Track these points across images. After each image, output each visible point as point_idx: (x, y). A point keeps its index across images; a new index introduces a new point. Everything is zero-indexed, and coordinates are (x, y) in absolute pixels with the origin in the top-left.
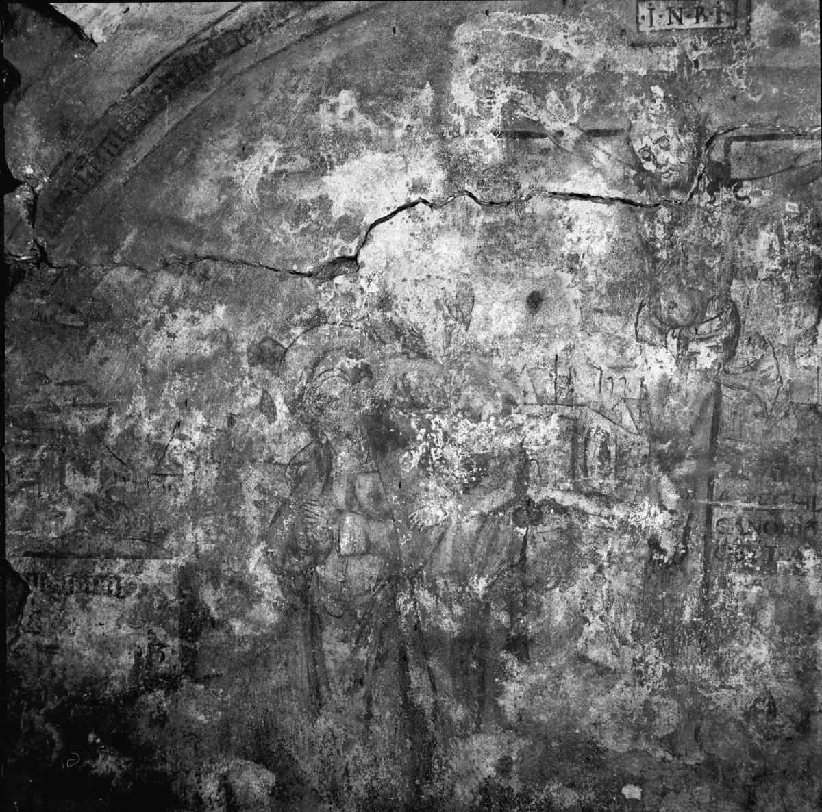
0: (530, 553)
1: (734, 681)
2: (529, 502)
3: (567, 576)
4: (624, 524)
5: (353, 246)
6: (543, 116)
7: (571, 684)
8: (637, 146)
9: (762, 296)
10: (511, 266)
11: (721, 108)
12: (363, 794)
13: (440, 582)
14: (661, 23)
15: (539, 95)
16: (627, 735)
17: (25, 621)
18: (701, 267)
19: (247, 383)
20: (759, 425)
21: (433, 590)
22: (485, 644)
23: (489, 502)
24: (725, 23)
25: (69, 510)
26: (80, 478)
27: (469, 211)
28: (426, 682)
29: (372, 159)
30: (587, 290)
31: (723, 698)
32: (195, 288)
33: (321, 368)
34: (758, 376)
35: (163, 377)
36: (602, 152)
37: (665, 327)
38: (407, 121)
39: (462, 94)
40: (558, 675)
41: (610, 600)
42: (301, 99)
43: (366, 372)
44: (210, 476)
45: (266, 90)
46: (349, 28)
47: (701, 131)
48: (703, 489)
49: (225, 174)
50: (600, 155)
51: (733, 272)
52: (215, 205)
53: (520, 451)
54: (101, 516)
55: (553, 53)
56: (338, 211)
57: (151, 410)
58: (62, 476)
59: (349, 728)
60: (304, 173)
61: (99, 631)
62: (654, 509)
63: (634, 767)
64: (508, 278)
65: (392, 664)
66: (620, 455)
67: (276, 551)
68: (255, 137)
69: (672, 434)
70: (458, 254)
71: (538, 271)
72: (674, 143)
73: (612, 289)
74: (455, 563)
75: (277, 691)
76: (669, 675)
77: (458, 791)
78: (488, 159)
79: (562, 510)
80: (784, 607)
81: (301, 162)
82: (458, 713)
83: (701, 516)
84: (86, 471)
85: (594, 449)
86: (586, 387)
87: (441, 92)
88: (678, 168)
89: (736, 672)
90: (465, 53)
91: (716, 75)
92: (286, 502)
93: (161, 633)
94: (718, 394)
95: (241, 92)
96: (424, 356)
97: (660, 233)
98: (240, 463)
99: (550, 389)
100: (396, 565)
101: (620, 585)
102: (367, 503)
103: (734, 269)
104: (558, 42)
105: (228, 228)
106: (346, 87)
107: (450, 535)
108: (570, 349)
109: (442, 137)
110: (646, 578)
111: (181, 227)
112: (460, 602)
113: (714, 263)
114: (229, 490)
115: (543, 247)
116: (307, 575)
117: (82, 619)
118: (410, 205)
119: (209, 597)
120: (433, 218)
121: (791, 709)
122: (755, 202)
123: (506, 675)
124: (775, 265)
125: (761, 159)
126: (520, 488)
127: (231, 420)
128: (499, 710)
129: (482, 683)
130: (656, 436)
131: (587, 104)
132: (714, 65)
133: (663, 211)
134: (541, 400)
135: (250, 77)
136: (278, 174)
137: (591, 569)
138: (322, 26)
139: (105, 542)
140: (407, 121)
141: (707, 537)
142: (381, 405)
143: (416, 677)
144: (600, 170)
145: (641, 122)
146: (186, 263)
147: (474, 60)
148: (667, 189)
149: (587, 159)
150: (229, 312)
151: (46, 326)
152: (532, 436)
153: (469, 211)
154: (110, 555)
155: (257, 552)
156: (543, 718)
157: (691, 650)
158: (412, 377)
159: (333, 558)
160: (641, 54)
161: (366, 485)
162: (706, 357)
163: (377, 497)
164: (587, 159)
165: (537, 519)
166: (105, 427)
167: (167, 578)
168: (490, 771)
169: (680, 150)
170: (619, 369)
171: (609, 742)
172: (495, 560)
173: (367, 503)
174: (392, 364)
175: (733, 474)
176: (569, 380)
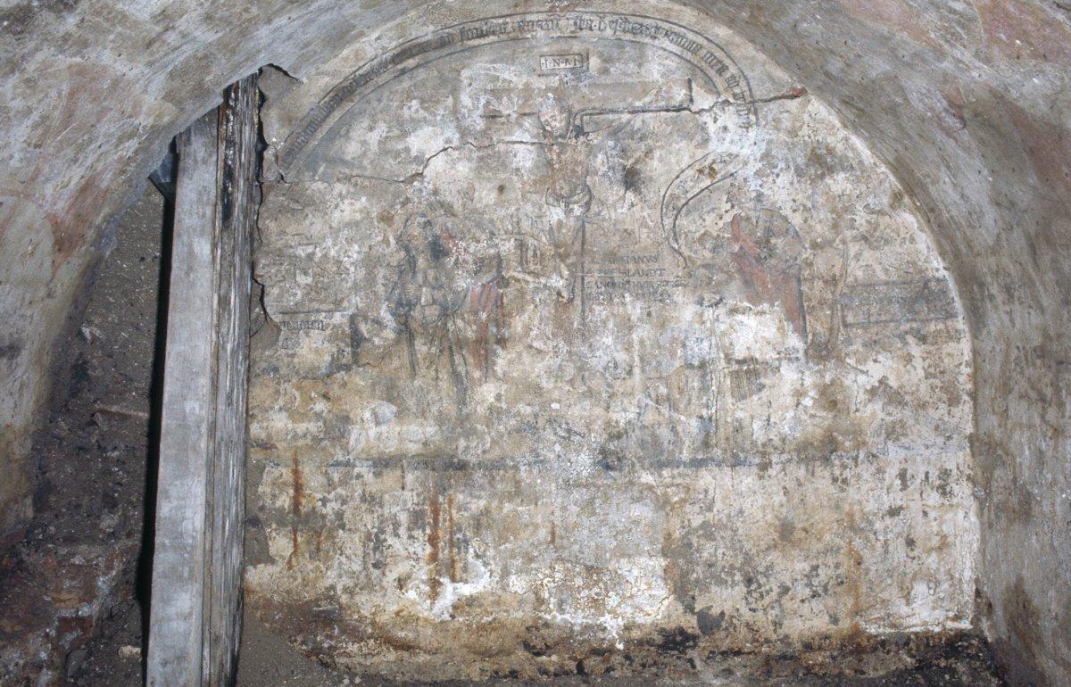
0: (505, 300)
1: (598, 354)
2: (503, 278)
3: (521, 310)
4: (545, 286)
5: (421, 168)
6: (501, 108)
7: (527, 359)
8: (543, 120)
9: (601, 183)
10: (490, 174)
11: (578, 102)
12: (437, 414)
13: (466, 316)
14: (550, 65)
15: (499, 99)
16: (553, 380)
17: (280, 343)
18: (573, 171)
19: (377, 231)
20: (602, 240)
21: (463, 319)
22: (486, 343)
23: (485, 279)
24: (578, 65)
25: (299, 292)
26: (303, 277)
27: (471, 151)
28: (462, 362)
29: (428, 130)
30: (524, 183)
31: (594, 361)
32: (352, 190)
33: (409, 222)
34: (601, 218)
35: (339, 230)
36: (527, 123)
37: (558, 198)
38: (442, 112)
39: (465, 99)
40: (520, 355)
41: (541, 320)
42: (396, 104)
43: (429, 223)
44: (362, 273)
45: (379, 101)
46: (415, 72)
47: (570, 112)
48: (579, 268)
49: (362, 139)
50: (526, 124)
51: (588, 173)
52: (360, 152)
53: (498, 255)
54: (313, 293)
55: (505, 80)
56: (414, 153)
57: (334, 245)
58: (295, 276)
59: (429, 385)
60: (398, 137)
61: (314, 346)
62: (559, 278)
63: (556, 395)
64: (489, 179)
65: (446, 353)
66: (542, 255)
67: (392, 305)
68: (375, 122)
69: (565, 245)
70: (467, 170)
71: (502, 176)
72: (558, 118)
73: (535, 182)
74: (472, 307)
75: (395, 369)
76: (569, 352)
77: (478, 409)
78: (478, 128)
79: (518, 280)
80: (618, 320)
81: (396, 132)
82: (477, 374)
83: (579, 280)
84: (306, 274)
85: (530, 253)
86: (525, 225)
87: (456, 100)
88: (561, 128)
89: (598, 349)
90: (466, 82)
91: (576, 88)
92: (396, 283)
93: (342, 345)
94: (583, 226)
95: (369, 102)
96: (454, 215)
97: (555, 157)
98: (375, 267)
99: (510, 227)
100: (447, 309)
101: (545, 313)
102: (433, 282)
103: (587, 171)
104: (506, 75)
105: (366, 163)
106: (415, 98)
107: (470, 294)
108: (518, 209)
109: (457, 118)
110: (556, 311)
111: (345, 163)
112: (475, 323)
113: (579, 169)
114: (370, 279)
115: (504, 165)
116: (407, 316)
117: (307, 340)
118: (445, 149)
119: (364, 328)
120: (456, 154)
121: (624, 365)
122: (595, 142)
123: (495, 354)
124: (605, 169)
125: (596, 123)
126: (499, 272)
127: (370, 248)
128: (494, 371)
129: (486, 359)
130: (557, 246)
131: (520, 102)
132: (573, 83)
133: (555, 147)
134: (506, 233)
135: (372, 95)
136: (387, 138)
137: (532, 306)
138: (403, 72)
139: (316, 305)
140: (442, 112)
141: (583, 290)
142: (436, 237)
143: (458, 359)
144: (527, 130)
145: (544, 109)
146: (348, 179)
147: (470, 85)
148: (556, 137)
149: (521, 126)
150: (368, 200)
151: (283, 210)
152: (502, 248)
153: (471, 151)
154: (318, 311)
155: (384, 307)
156: (515, 375)
157: (578, 341)
158: (449, 225)
159: (418, 307)
160: (543, 80)
161: (431, 273)
162: (577, 211)
163: (436, 279)
164: (521, 126)
165: (507, 285)
166: (313, 254)
167: (345, 320)
168: (492, 400)
169: (561, 121)
170: (540, 217)
171: (544, 384)
172: (490, 304)
173: (433, 282)
174: (440, 219)
175: (593, 262)
176: (518, 223)
